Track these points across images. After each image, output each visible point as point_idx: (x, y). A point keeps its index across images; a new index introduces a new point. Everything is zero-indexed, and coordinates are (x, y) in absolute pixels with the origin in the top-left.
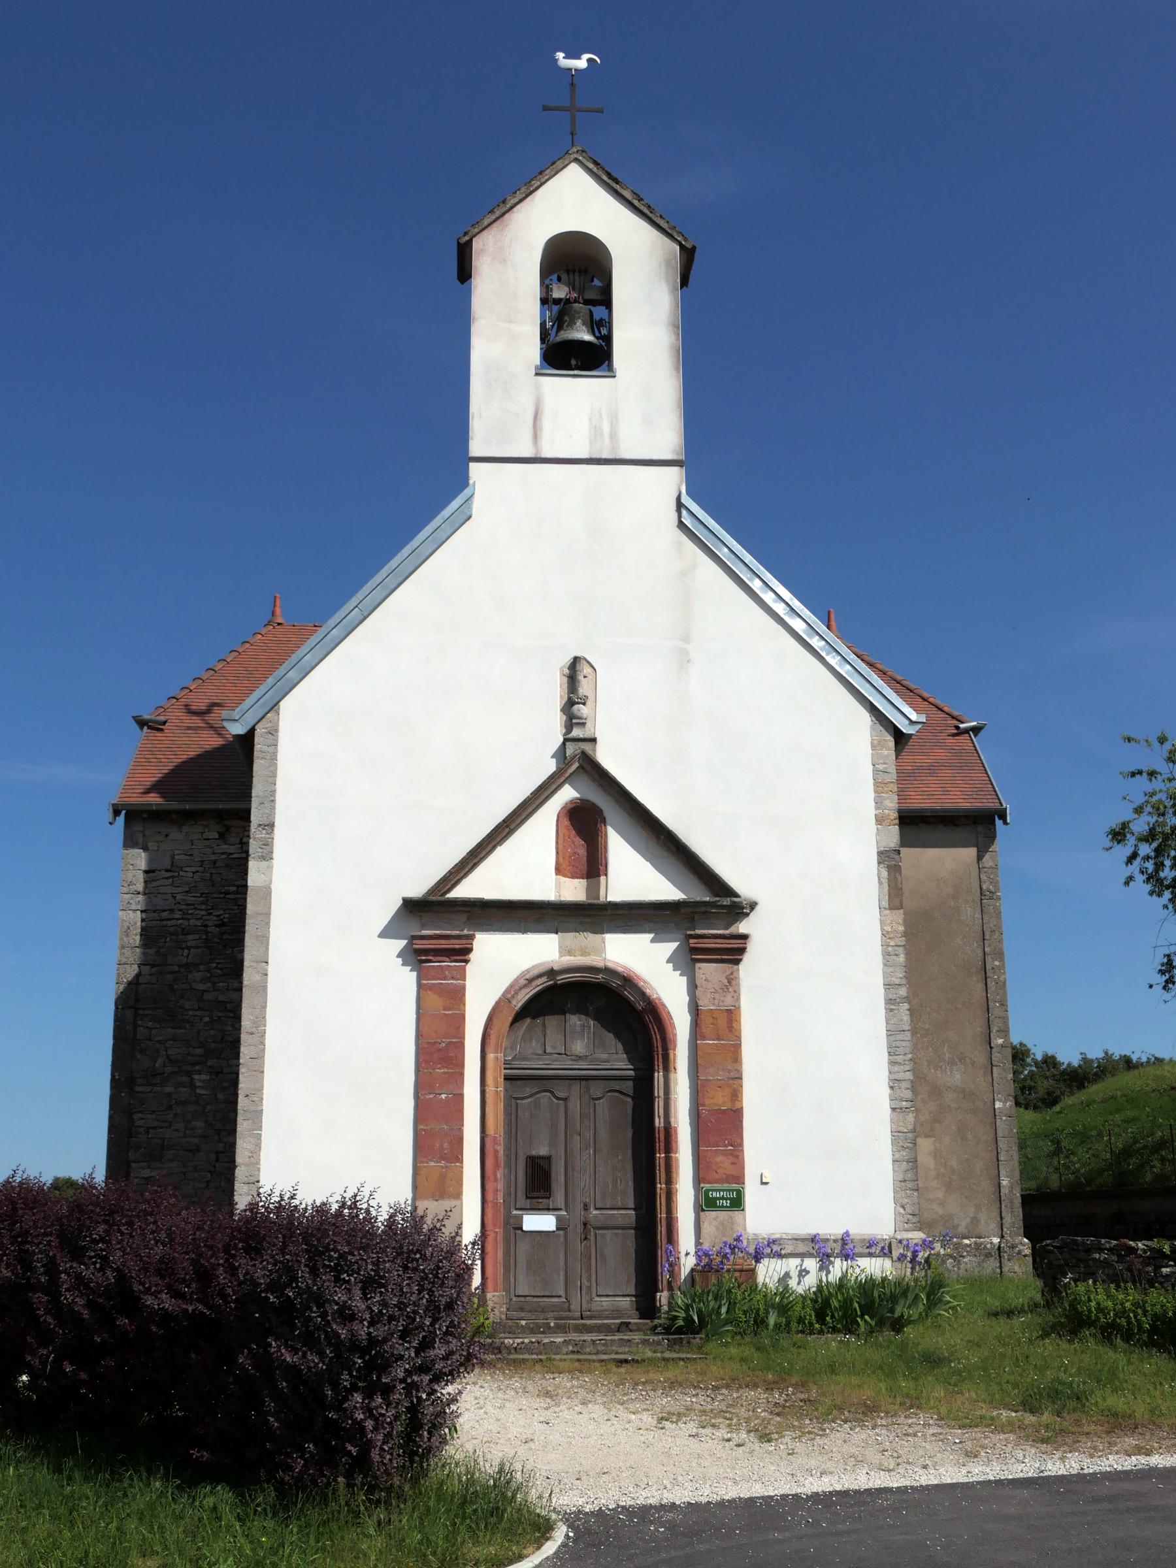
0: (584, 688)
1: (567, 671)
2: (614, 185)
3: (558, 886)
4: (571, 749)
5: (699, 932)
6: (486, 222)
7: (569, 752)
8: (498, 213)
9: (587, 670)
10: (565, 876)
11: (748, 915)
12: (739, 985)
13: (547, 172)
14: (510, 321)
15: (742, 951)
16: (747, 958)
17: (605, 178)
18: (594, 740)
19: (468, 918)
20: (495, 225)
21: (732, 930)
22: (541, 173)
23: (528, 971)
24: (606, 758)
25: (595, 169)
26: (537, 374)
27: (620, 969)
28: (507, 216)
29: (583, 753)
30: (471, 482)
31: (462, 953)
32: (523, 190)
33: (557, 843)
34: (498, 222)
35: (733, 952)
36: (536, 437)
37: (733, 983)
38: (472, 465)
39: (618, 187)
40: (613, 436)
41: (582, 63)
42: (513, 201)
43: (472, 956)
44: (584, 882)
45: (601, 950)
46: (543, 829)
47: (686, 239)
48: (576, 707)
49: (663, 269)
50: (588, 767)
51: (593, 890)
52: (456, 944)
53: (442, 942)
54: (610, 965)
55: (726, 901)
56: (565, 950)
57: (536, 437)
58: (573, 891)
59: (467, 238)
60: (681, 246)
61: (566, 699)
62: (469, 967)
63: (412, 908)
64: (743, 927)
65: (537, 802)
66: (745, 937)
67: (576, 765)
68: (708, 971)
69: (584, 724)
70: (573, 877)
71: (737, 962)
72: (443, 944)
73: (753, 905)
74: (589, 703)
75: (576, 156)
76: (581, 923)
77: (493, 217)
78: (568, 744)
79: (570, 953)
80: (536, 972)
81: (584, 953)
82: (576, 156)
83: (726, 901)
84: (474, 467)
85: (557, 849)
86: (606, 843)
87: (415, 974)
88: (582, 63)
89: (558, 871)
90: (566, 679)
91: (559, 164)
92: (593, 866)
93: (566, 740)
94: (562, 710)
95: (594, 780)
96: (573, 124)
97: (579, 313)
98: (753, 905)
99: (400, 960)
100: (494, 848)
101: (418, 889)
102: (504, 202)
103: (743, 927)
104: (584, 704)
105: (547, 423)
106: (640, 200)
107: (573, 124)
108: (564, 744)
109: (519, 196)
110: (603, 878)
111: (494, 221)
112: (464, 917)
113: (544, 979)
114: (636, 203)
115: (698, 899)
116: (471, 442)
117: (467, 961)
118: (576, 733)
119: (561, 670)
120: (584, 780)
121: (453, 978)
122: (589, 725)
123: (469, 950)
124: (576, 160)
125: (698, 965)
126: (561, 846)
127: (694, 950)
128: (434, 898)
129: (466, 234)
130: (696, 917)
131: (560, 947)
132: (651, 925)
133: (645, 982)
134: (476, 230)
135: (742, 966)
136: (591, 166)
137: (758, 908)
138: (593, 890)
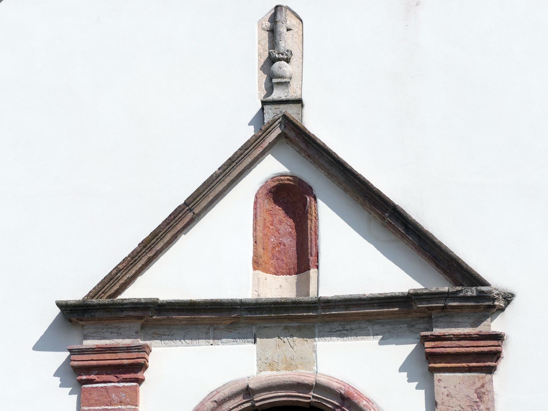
0: (287, 42)
1: (267, 24)
3: (257, 283)
4: (271, 113)
5: (437, 331)
7: (268, 118)
9: (291, 21)
10: (267, 271)
11: (502, 310)
12: (493, 401)
15: (496, 355)
16: (502, 366)
18: (299, 102)
19: (143, 327)
21: (483, 328)
23: (217, 391)
24: (314, 123)
27: (335, 385)
29: (285, 117)
31: (132, 370)
33: (255, 230)
35: (485, 357)
37: (485, 398)
43: (147, 375)
44: (293, 278)
45: (310, 361)
46: (238, 211)
48: (277, 64)
50: (291, 134)
51: (303, 286)
52: (125, 359)
53: (107, 356)
54: (323, 380)
55: (472, 292)
56: (265, 363)
58: (279, 287)
61: (266, 55)
62: (143, 389)
63: (74, 314)
64: (495, 325)
65: (228, 180)
66: (498, 337)
67: (278, 131)
68: (450, 382)
69: (286, 84)
70: (277, 273)
71: (491, 370)
72: (108, 359)
73: (508, 298)
74: (293, 60)
76: (286, 328)
78: (266, 107)
79: (271, 366)
80: (227, 392)
81: (289, 367)
83: (472, 292)
85: (255, 237)
86: (317, 227)
87: (75, 397)
89: (257, 264)
90: (266, 34)
92: (303, 258)
93: (264, 103)
94: (263, 68)
95: (300, 151)
98: (508, 298)
99: (57, 380)
100: (175, 238)
101: (77, 293)
103: (495, 325)
104: (288, 61)
108: (263, 109)
110: (313, 272)
112: (137, 325)
113: (239, 400)
115: (434, 289)
117: (140, 381)
118: (278, 94)
119: (260, 22)
120: (289, 151)
121: (121, 403)
122: (294, 84)
123: (142, 367)
125: (437, 376)
126: (260, 234)
127: (431, 357)
128: (95, 301)
130: (434, 314)
131: (259, 359)
132: (376, 327)
133: (368, 400)
135: (497, 378)
137: (515, 302)
138: (303, 286)
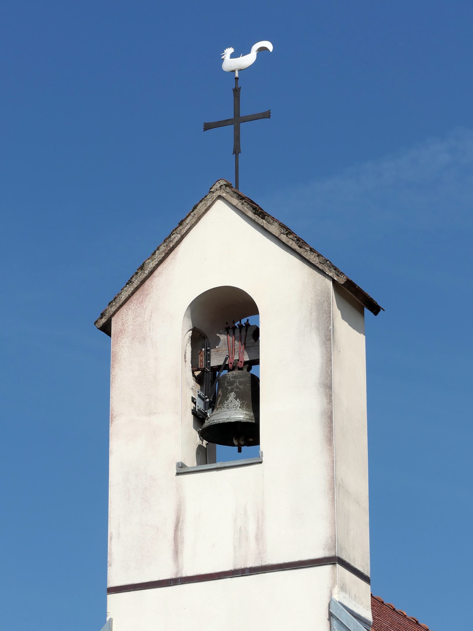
2: (260, 221)
6: (123, 297)
8: (136, 282)
13: (188, 221)
14: (150, 414)
17: (250, 214)
20: (134, 297)
22: (181, 224)
25: (240, 206)
26: (178, 474)
28: (147, 282)
30: (108, 619)
32: (162, 248)
34: (138, 293)
36: (176, 552)
38: (112, 598)
39: (263, 222)
40: (259, 537)
41: (249, 59)
42: (152, 265)
47: (339, 273)
49: (314, 315)
57: (176, 552)
59: (104, 320)
60: (334, 281)
75: (218, 193)
77: (131, 289)
82: (218, 193)
84: (113, 600)
88: (249, 59)
91: (201, 208)
96: (237, 139)
97: (231, 383)
102: (142, 268)
105: (188, 534)
106: (289, 232)
107: (237, 139)
109: (158, 256)
111: (133, 293)
114: (284, 238)
116: (109, 568)
124: (220, 197)
129: (102, 315)
134: (113, 309)
136: (235, 201)
